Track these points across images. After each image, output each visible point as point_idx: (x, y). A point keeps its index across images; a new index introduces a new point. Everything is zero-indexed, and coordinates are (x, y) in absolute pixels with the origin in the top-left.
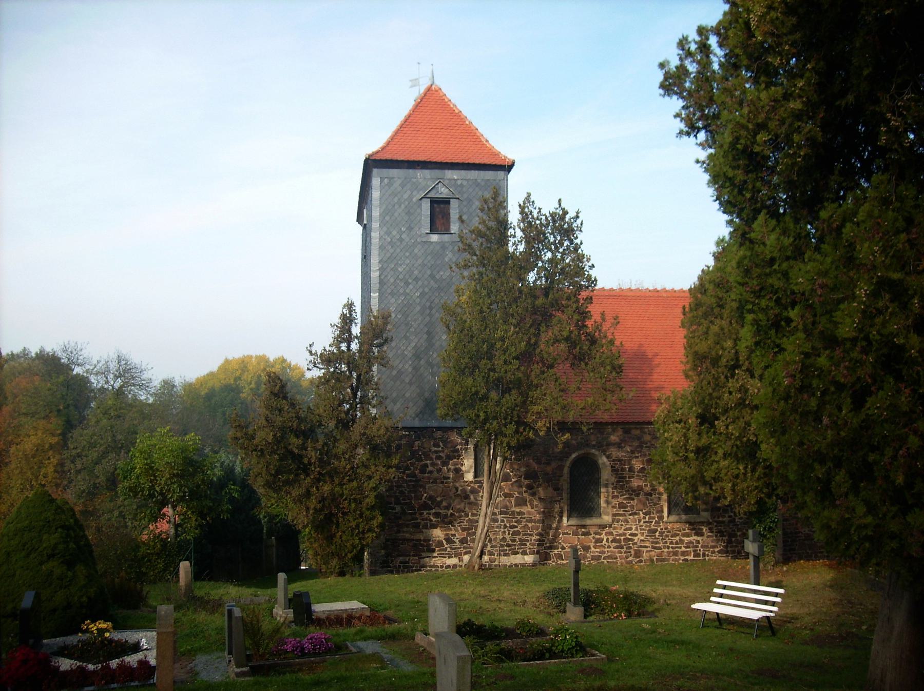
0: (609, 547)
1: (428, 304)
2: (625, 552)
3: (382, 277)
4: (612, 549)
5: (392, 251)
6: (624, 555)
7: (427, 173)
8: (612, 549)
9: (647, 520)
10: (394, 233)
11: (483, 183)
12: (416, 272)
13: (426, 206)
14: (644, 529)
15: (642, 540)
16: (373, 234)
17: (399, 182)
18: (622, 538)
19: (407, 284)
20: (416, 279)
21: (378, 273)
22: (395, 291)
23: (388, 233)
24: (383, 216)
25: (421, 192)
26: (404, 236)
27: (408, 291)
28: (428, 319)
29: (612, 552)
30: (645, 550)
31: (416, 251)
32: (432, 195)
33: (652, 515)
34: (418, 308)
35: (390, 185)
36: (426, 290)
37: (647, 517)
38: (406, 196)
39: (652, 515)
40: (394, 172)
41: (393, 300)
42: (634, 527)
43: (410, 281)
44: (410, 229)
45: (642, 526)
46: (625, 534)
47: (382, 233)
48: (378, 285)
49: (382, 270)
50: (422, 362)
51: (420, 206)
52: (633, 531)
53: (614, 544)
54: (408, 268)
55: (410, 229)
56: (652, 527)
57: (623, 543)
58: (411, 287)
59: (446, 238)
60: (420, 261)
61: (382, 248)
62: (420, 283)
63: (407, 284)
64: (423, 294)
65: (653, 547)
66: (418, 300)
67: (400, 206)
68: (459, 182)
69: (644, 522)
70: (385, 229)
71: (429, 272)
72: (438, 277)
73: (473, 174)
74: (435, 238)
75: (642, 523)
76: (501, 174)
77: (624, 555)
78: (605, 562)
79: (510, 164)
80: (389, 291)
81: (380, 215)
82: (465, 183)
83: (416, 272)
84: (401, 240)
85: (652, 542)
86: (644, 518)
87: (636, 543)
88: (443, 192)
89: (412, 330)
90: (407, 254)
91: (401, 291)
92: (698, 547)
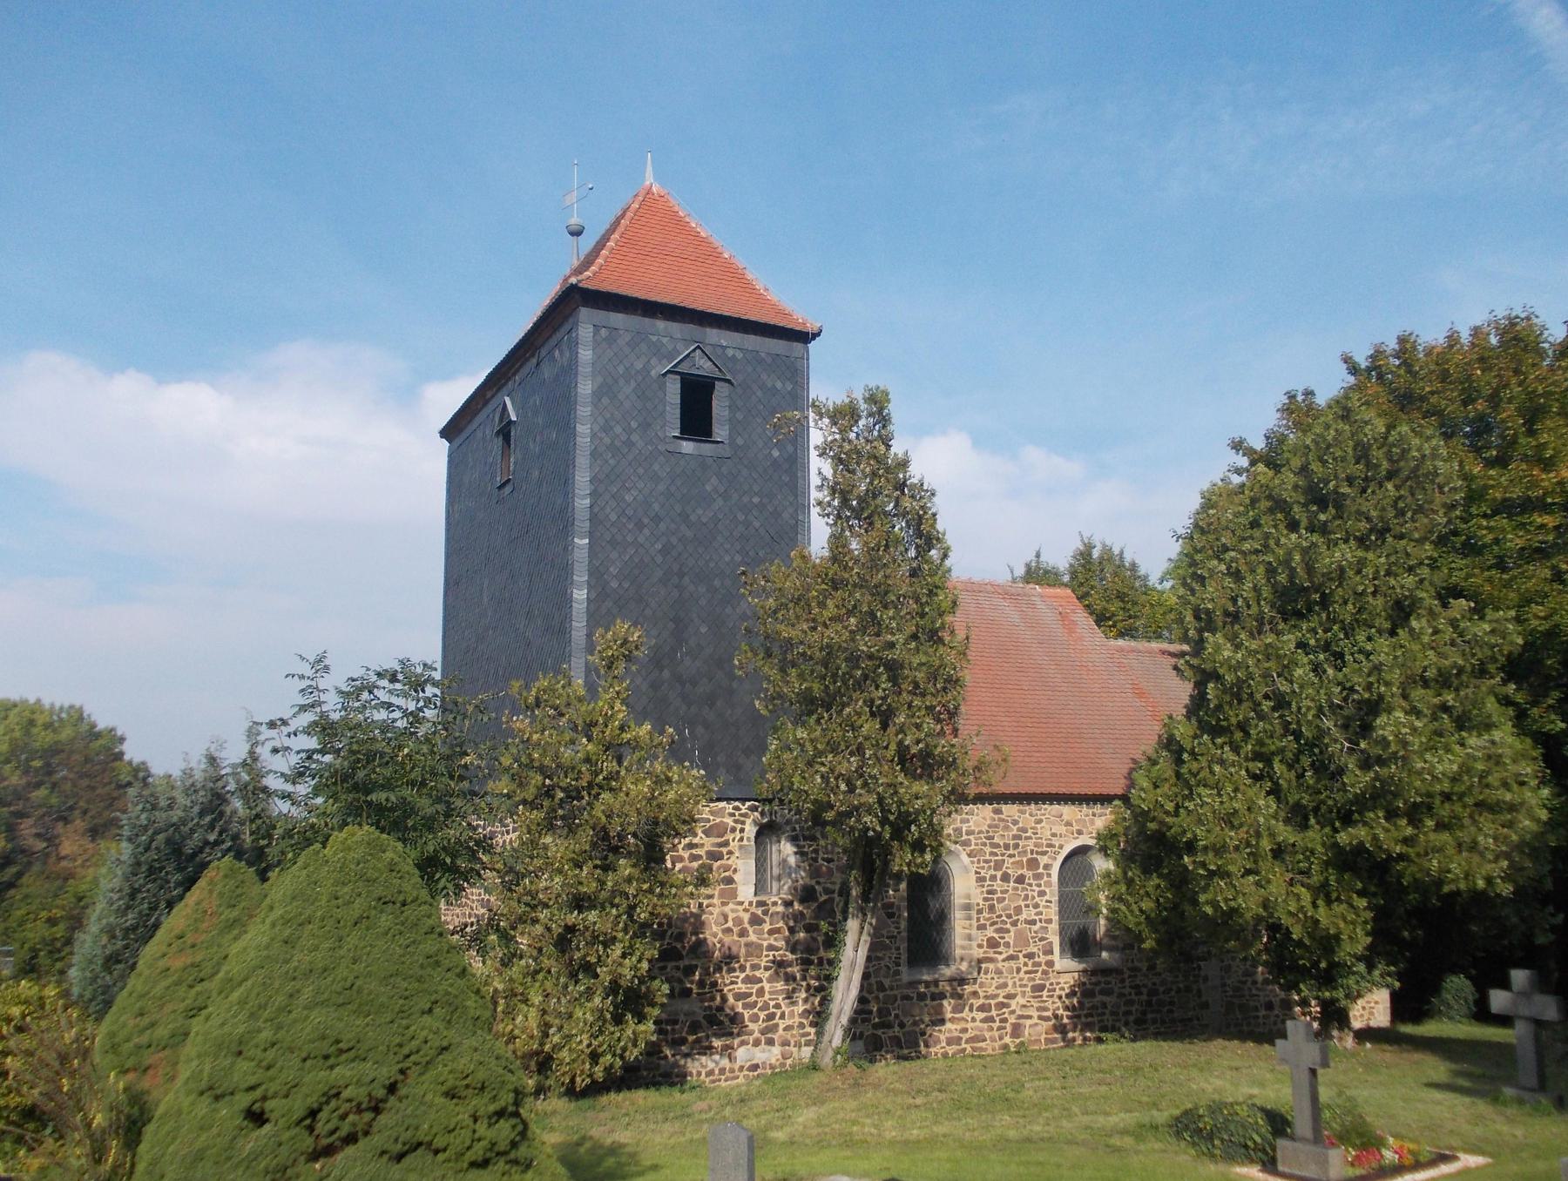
0: (974, 1020)
1: (676, 567)
2: (999, 1029)
3: (596, 510)
4: (978, 1023)
5: (612, 462)
6: (996, 1034)
7: (675, 328)
8: (978, 1023)
9: (1030, 968)
10: (618, 430)
11: (769, 360)
12: (656, 506)
13: (674, 389)
14: (1025, 986)
15: (1024, 1006)
16: (579, 428)
17: (628, 337)
18: (993, 1002)
19: (640, 526)
20: (657, 519)
21: (587, 501)
22: (619, 538)
23: (606, 428)
24: (598, 395)
25: (664, 361)
26: (635, 437)
27: (641, 539)
28: (675, 593)
29: (977, 1028)
30: (1028, 1022)
31: (656, 467)
32: (683, 368)
33: (1037, 959)
34: (659, 573)
35: (611, 340)
36: (674, 540)
37: (1030, 963)
38: (639, 365)
39: (1037, 959)
40: (617, 319)
41: (614, 555)
42: (1010, 983)
43: (646, 521)
44: (645, 426)
45: (1021, 980)
46: (996, 996)
47: (596, 428)
48: (587, 524)
49: (594, 494)
50: (666, 674)
51: (662, 387)
52: (1010, 989)
53: (982, 1015)
54: (640, 497)
55: (645, 426)
56: (1038, 982)
57: (994, 1013)
58: (646, 531)
59: (706, 449)
60: (661, 487)
61: (594, 455)
62: (662, 526)
63: (640, 526)
64: (665, 551)
65: (1040, 1018)
66: (659, 559)
67: (628, 382)
68: (730, 352)
69: (1026, 973)
70: (601, 420)
71: (678, 508)
72: (693, 518)
73: (752, 341)
74: (688, 447)
75: (1022, 974)
76: (798, 346)
77: (996, 1034)
78: (969, 1050)
79: (816, 331)
80: (608, 537)
81: (594, 393)
82: (739, 355)
83: (656, 506)
84: (630, 444)
85: (1039, 1009)
86: (1026, 964)
87: (1013, 1012)
88: (703, 367)
89: (648, 612)
90: (641, 471)
91: (629, 538)
92: (1104, 1014)
